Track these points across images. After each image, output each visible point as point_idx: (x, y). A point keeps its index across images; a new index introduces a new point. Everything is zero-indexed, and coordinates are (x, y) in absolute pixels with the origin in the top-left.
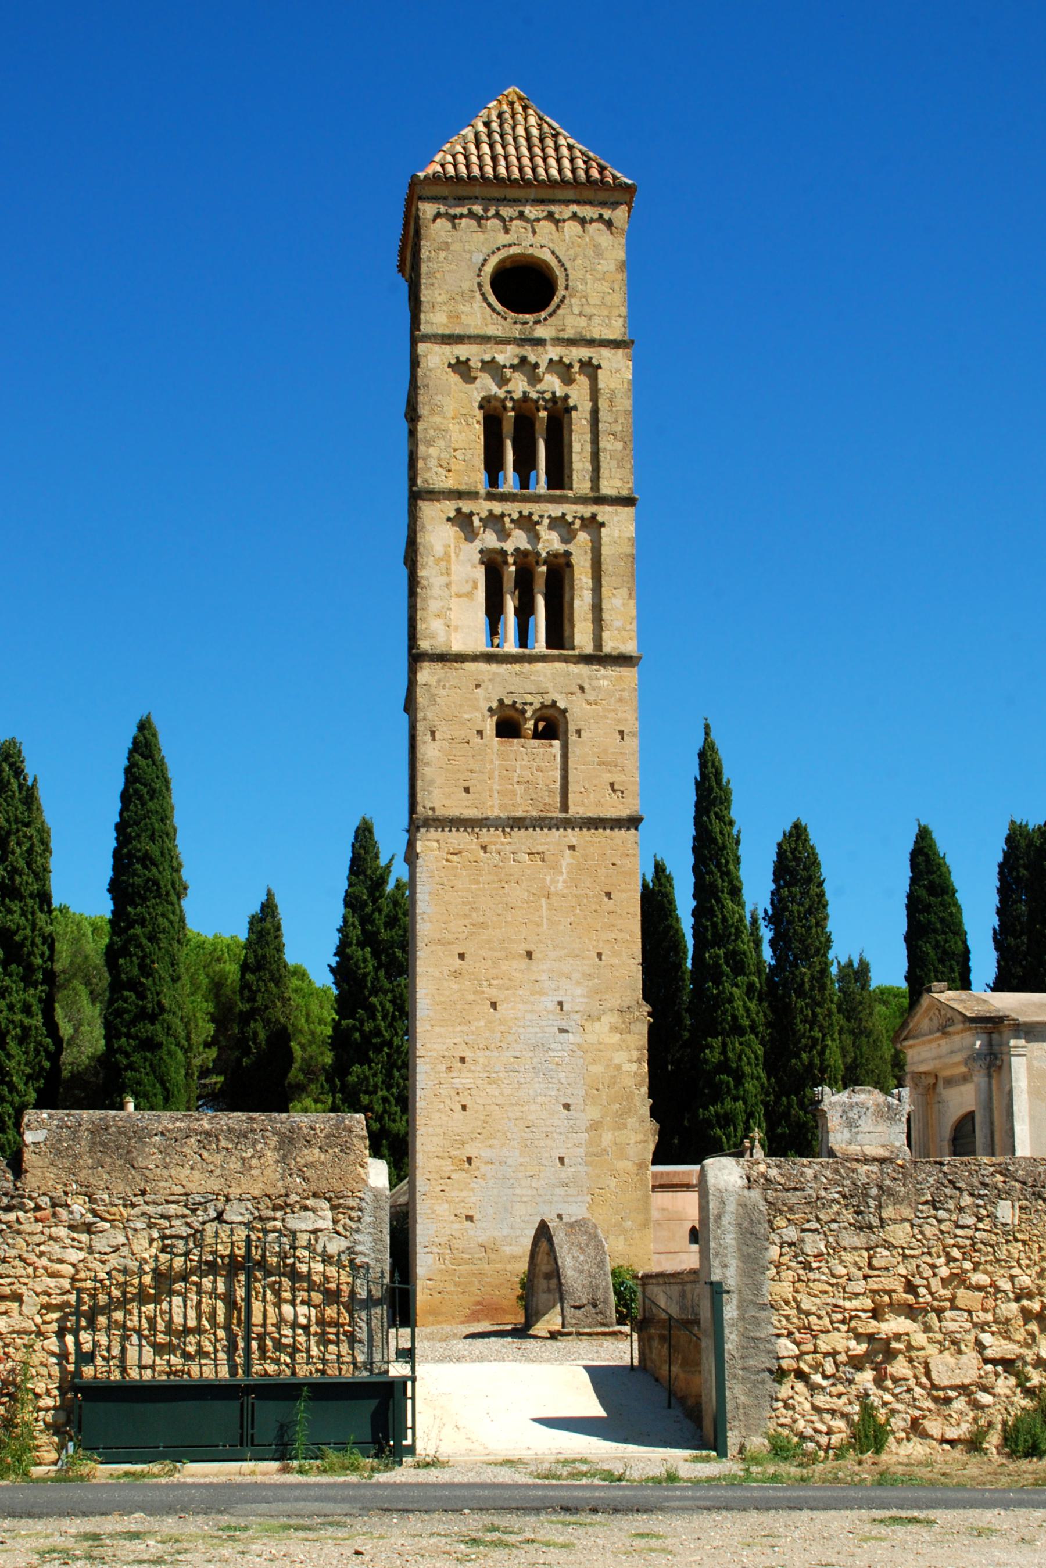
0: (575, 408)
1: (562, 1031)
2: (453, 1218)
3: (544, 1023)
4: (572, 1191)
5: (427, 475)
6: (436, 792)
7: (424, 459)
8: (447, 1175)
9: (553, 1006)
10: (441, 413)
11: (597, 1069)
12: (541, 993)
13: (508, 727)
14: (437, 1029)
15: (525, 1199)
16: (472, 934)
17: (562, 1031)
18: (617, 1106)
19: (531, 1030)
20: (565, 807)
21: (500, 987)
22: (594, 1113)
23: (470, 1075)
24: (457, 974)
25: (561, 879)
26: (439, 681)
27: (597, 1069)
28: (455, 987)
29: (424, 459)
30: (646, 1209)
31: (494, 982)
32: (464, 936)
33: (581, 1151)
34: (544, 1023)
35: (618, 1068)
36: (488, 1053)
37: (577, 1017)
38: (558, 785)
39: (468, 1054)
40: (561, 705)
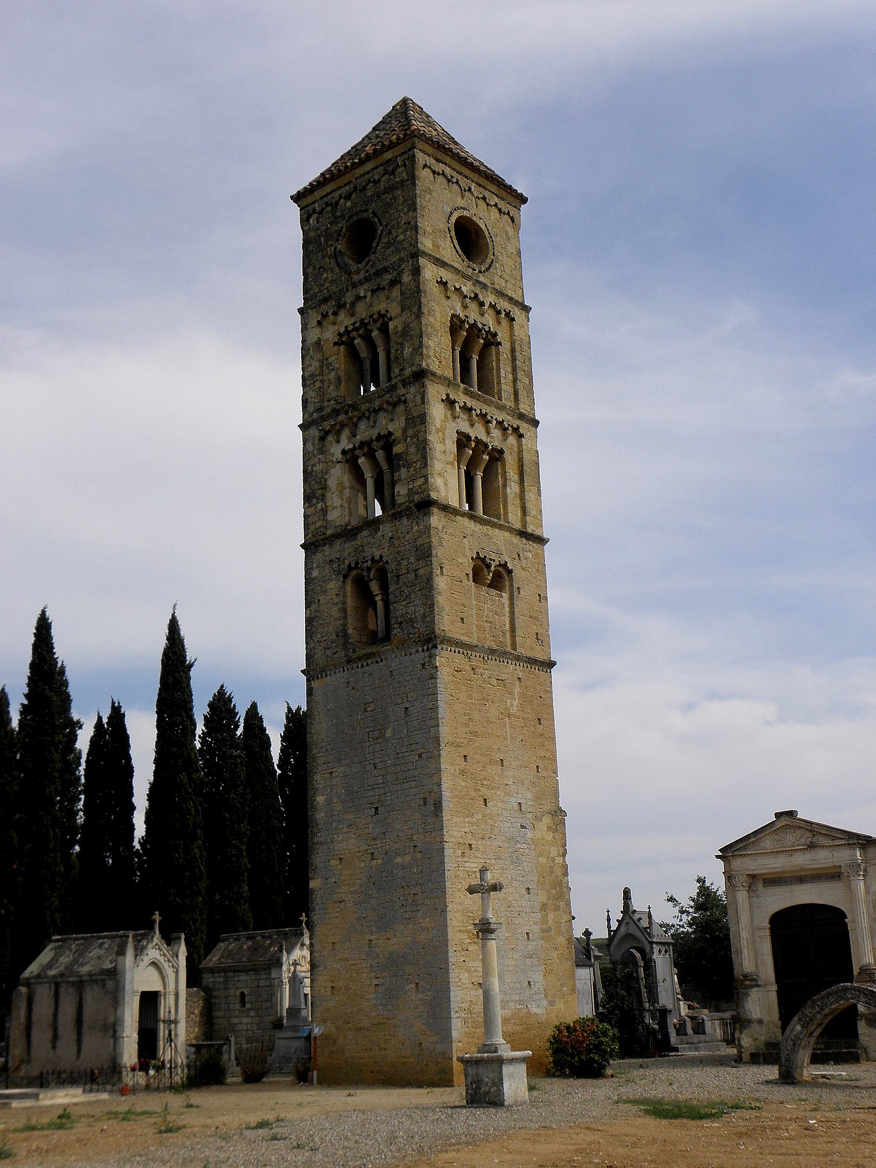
0: (499, 344)
1: (523, 827)
2: (471, 985)
3: (513, 820)
4: (535, 961)
5: (429, 361)
6: (446, 617)
7: (427, 348)
8: (465, 947)
9: (516, 807)
10: (434, 315)
11: (542, 860)
12: (509, 794)
13: (477, 576)
14: (455, 819)
15: (510, 969)
16: (471, 740)
17: (523, 827)
18: (554, 892)
19: (507, 825)
20: (514, 646)
21: (489, 787)
22: (542, 897)
23: (475, 860)
24: (463, 772)
25: (516, 703)
26: (443, 527)
27: (542, 860)
28: (463, 784)
29: (427, 348)
30: (573, 976)
31: (485, 782)
32: (466, 741)
33: (537, 928)
34: (513, 820)
35: (553, 860)
36: (484, 842)
37: (529, 816)
38: (508, 627)
39: (473, 842)
40: (510, 566)
